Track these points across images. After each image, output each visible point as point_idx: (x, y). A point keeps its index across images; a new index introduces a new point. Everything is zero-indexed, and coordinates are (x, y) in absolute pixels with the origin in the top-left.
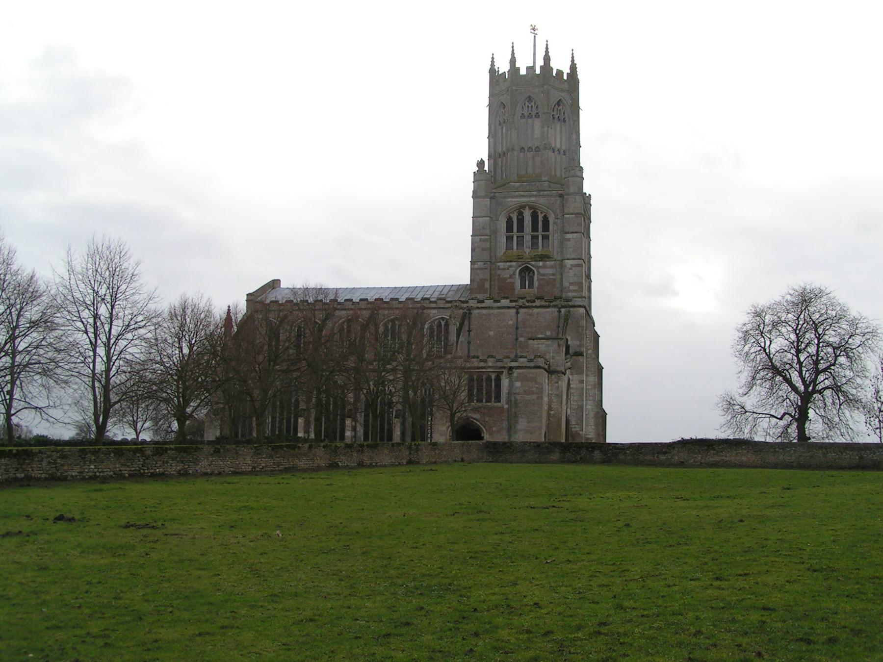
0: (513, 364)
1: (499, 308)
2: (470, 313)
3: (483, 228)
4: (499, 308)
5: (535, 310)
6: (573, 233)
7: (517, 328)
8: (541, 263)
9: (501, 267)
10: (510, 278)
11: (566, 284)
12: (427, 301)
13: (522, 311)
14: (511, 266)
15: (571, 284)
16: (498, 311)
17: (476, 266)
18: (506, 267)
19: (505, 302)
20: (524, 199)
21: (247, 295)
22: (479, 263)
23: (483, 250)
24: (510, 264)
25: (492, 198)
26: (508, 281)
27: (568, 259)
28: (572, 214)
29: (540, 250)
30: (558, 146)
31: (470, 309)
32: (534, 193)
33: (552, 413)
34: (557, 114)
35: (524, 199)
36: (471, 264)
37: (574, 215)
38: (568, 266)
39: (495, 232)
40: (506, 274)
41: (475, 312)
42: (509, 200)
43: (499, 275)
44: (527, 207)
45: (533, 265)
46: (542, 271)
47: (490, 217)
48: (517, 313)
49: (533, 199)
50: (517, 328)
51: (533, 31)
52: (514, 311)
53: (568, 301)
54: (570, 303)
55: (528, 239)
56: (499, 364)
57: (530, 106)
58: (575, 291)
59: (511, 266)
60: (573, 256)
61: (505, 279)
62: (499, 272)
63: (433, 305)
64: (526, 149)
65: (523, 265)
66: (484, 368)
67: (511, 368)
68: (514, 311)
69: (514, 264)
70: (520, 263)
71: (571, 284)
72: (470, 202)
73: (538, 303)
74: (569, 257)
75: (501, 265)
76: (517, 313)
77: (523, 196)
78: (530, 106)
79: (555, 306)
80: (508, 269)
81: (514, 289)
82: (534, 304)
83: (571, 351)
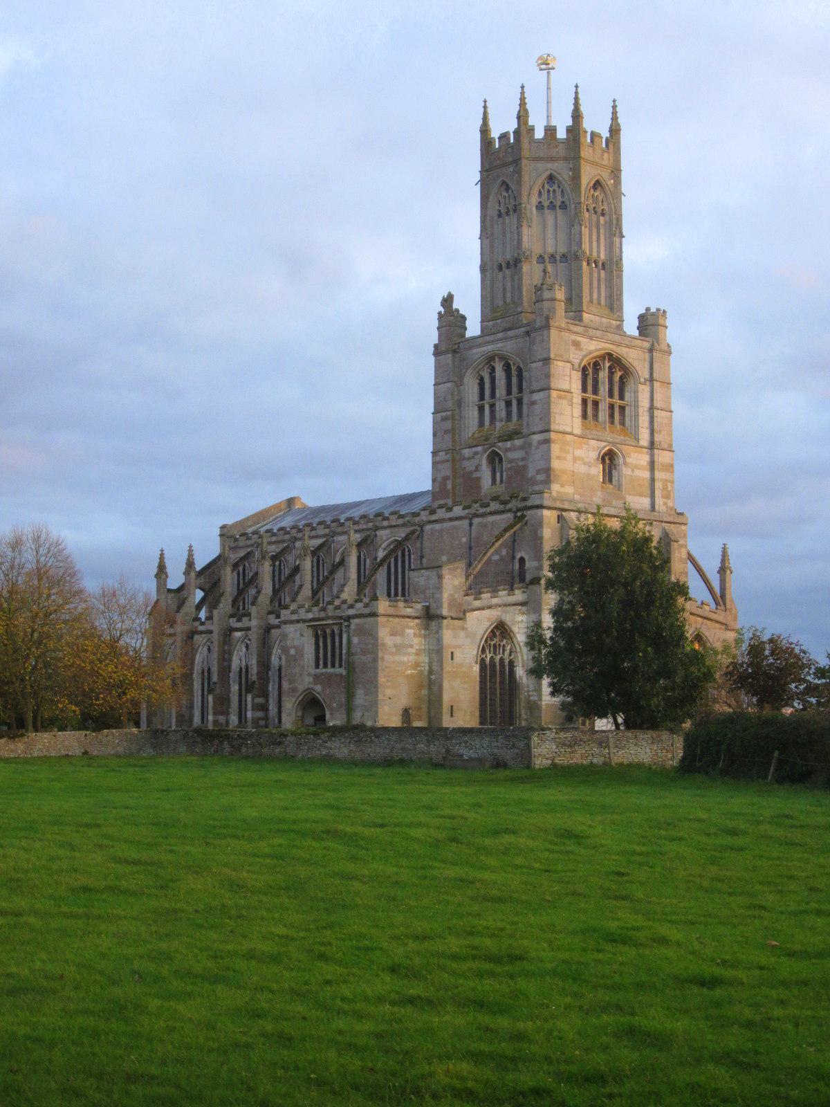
0: (351, 612)
1: (451, 519)
2: (422, 531)
3: (445, 400)
4: (451, 519)
5: (491, 519)
6: (539, 391)
7: (470, 548)
8: (509, 444)
9: (466, 456)
10: (476, 471)
11: (531, 473)
12: (380, 518)
13: (476, 521)
14: (476, 453)
15: (538, 472)
16: (451, 523)
17: (438, 459)
18: (471, 455)
19: (458, 511)
20: (490, 348)
21: (221, 528)
22: (440, 453)
23: (446, 432)
24: (474, 449)
25: (454, 351)
26: (474, 476)
27: (534, 434)
28: (540, 361)
29: (512, 426)
30: (550, 250)
31: (421, 526)
32: (500, 335)
33: (433, 677)
34: (548, 199)
35: (490, 348)
36: (433, 456)
37: (541, 363)
38: (535, 443)
39: (459, 403)
40: (470, 465)
41: (428, 528)
42: (475, 351)
43: (465, 468)
44: (497, 359)
45: (501, 447)
46: (512, 455)
47: (454, 382)
48: (471, 525)
49: (500, 345)
50: (470, 548)
51: (543, 67)
52: (466, 522)
53: (525, 499)
54: (529, 503)
55: (500, 406)
56: (338, 613)
57: (507, 195)
58: (541, 482)
59: (476, 453)
60: (540, 428)
61: (471, 473)
62: (466, 463)
63: (385, 523)
64: (558, 258)
65: (488, 448)
66: (323, 619)
67: (348, 618)
68: (466, 522)
69: (479, 449)
70: (487, 446)
71: (538, 472)
72: (430, 361)
73: (494, 506)
74: (536, 429)
75: (467, 452)
76: (471, 525)
77: (488, 342)
78: (551, 189)
79: (510, 510)
80: (473, 458)
81: (479, 488)
82: (488, 510)
83: (528, 577)
